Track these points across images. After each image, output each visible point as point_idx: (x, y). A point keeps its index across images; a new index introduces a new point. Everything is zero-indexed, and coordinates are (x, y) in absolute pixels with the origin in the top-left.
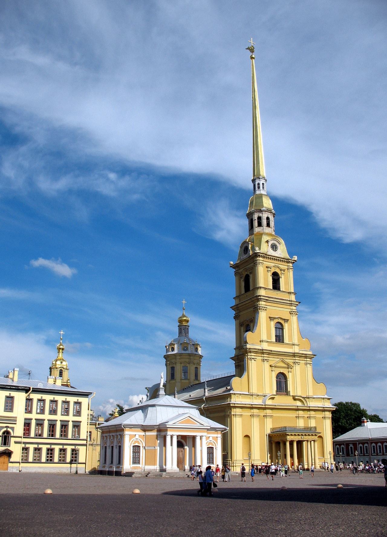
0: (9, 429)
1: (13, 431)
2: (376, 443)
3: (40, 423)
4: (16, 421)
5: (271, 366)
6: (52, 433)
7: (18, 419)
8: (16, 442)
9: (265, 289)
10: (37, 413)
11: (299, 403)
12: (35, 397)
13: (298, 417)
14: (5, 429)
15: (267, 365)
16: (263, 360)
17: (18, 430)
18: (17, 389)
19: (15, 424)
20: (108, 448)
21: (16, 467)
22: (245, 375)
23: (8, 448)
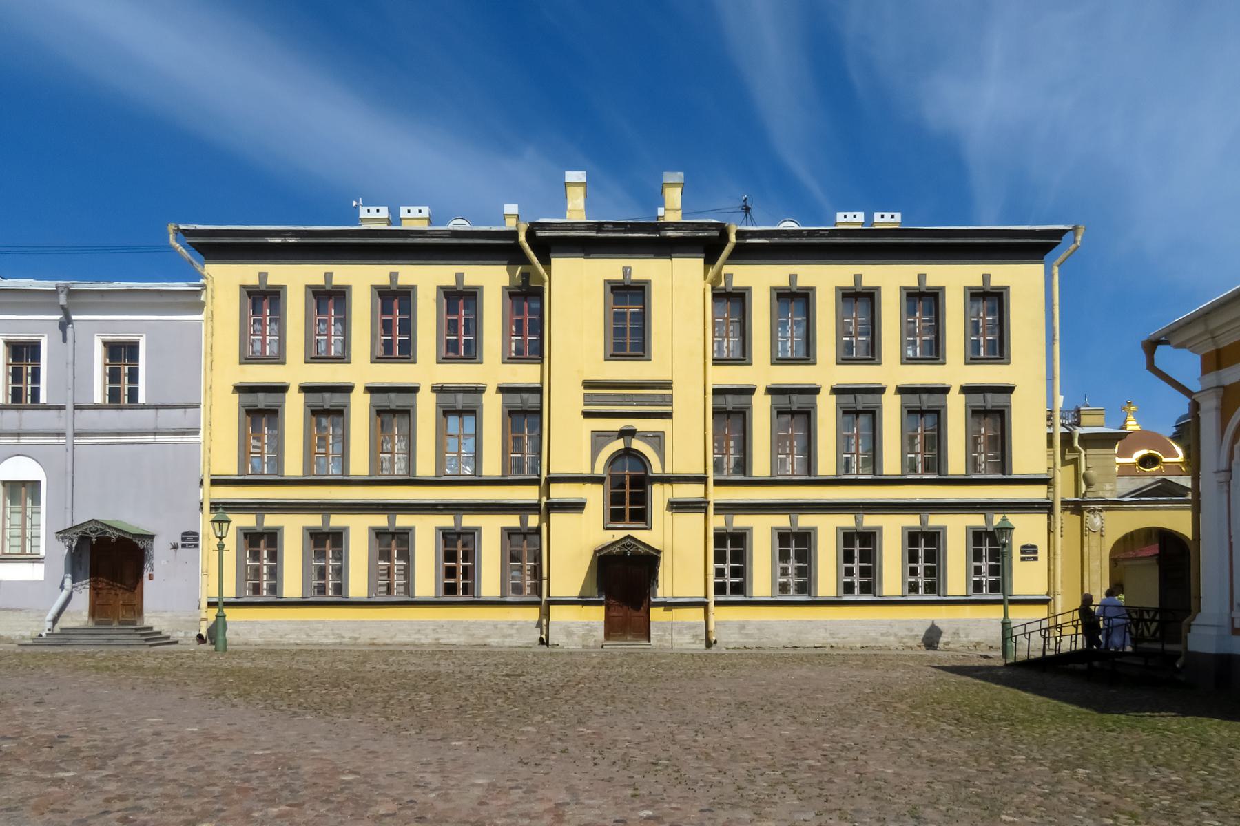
0: (637, 444)
3: (795, 408)
4: (669, 400)
7: (677, 391)
8: (677, 506)
10: (778, 361)
12: (760, 280)
14: (619, 444)
17: (686, 443)
18: (660, 243)
19: (668, 415)
21: (691, 627)
23: (640, 535)
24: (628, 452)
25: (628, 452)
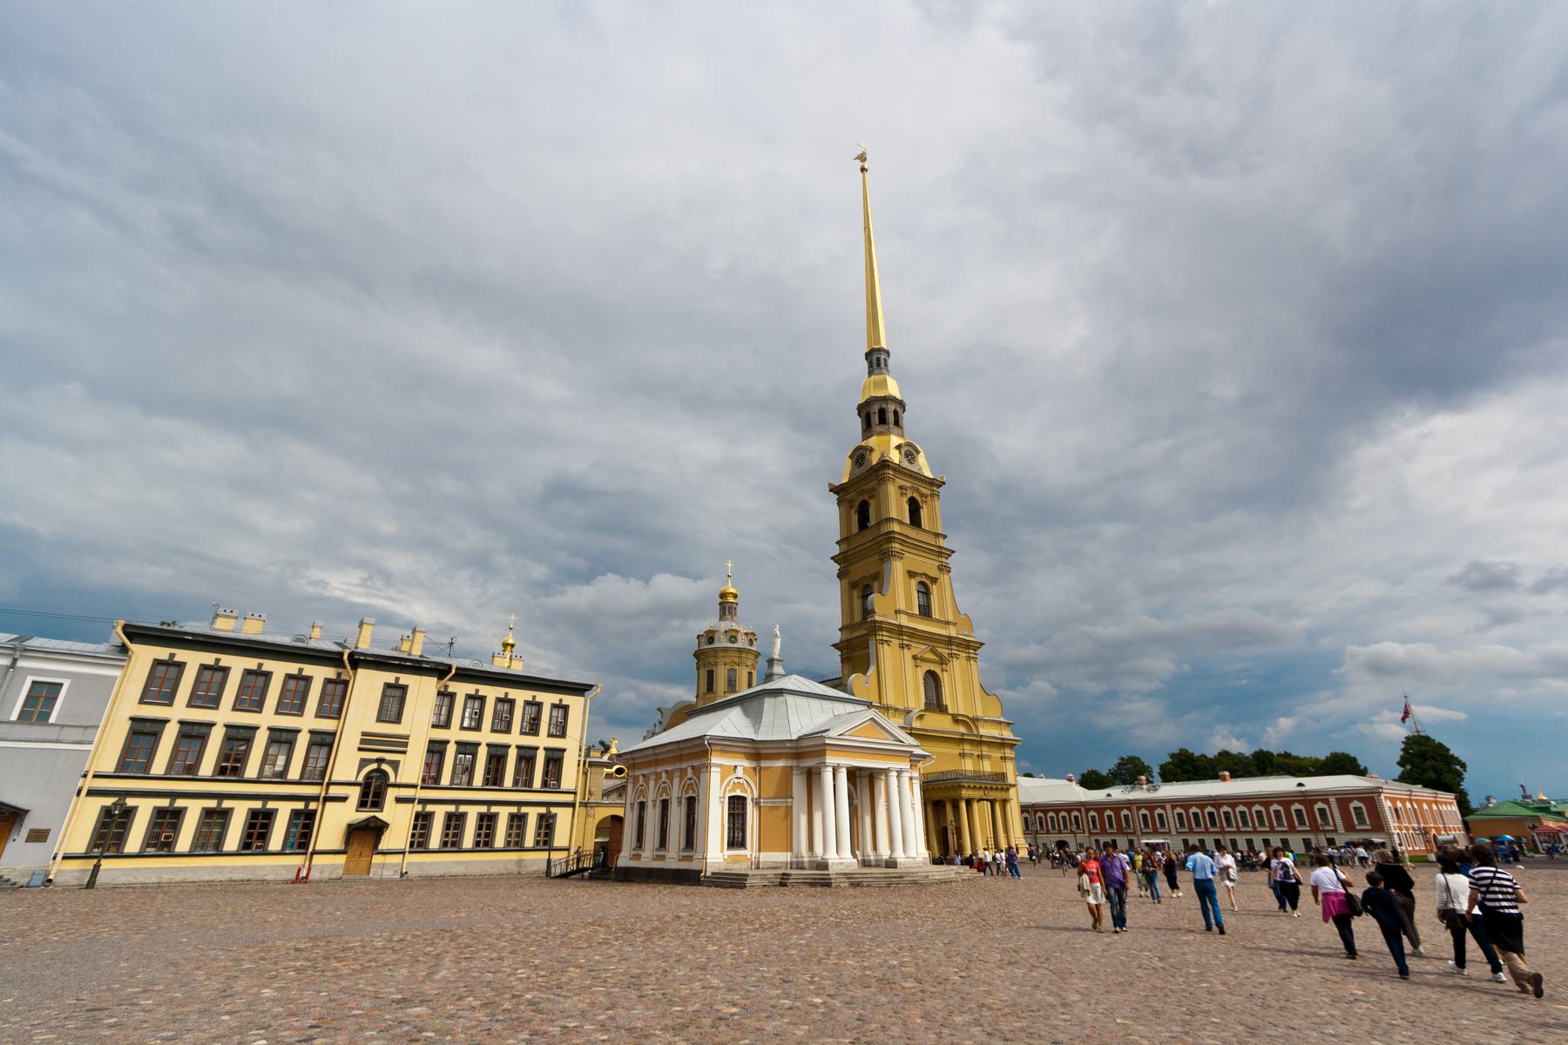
0: (385, 767)
1: (396, 770)
2: (1057, 812)
5: (915, 657)
6: (494, 777)
9: (901, 522)
11: (962, 729)
13: (962, 755)
14: (375, 766)
15: (908, 654)
16: (902, 647)
20: (650, 805)
22: (872, 670)
24: (379, 770)
25: (379, 770)
